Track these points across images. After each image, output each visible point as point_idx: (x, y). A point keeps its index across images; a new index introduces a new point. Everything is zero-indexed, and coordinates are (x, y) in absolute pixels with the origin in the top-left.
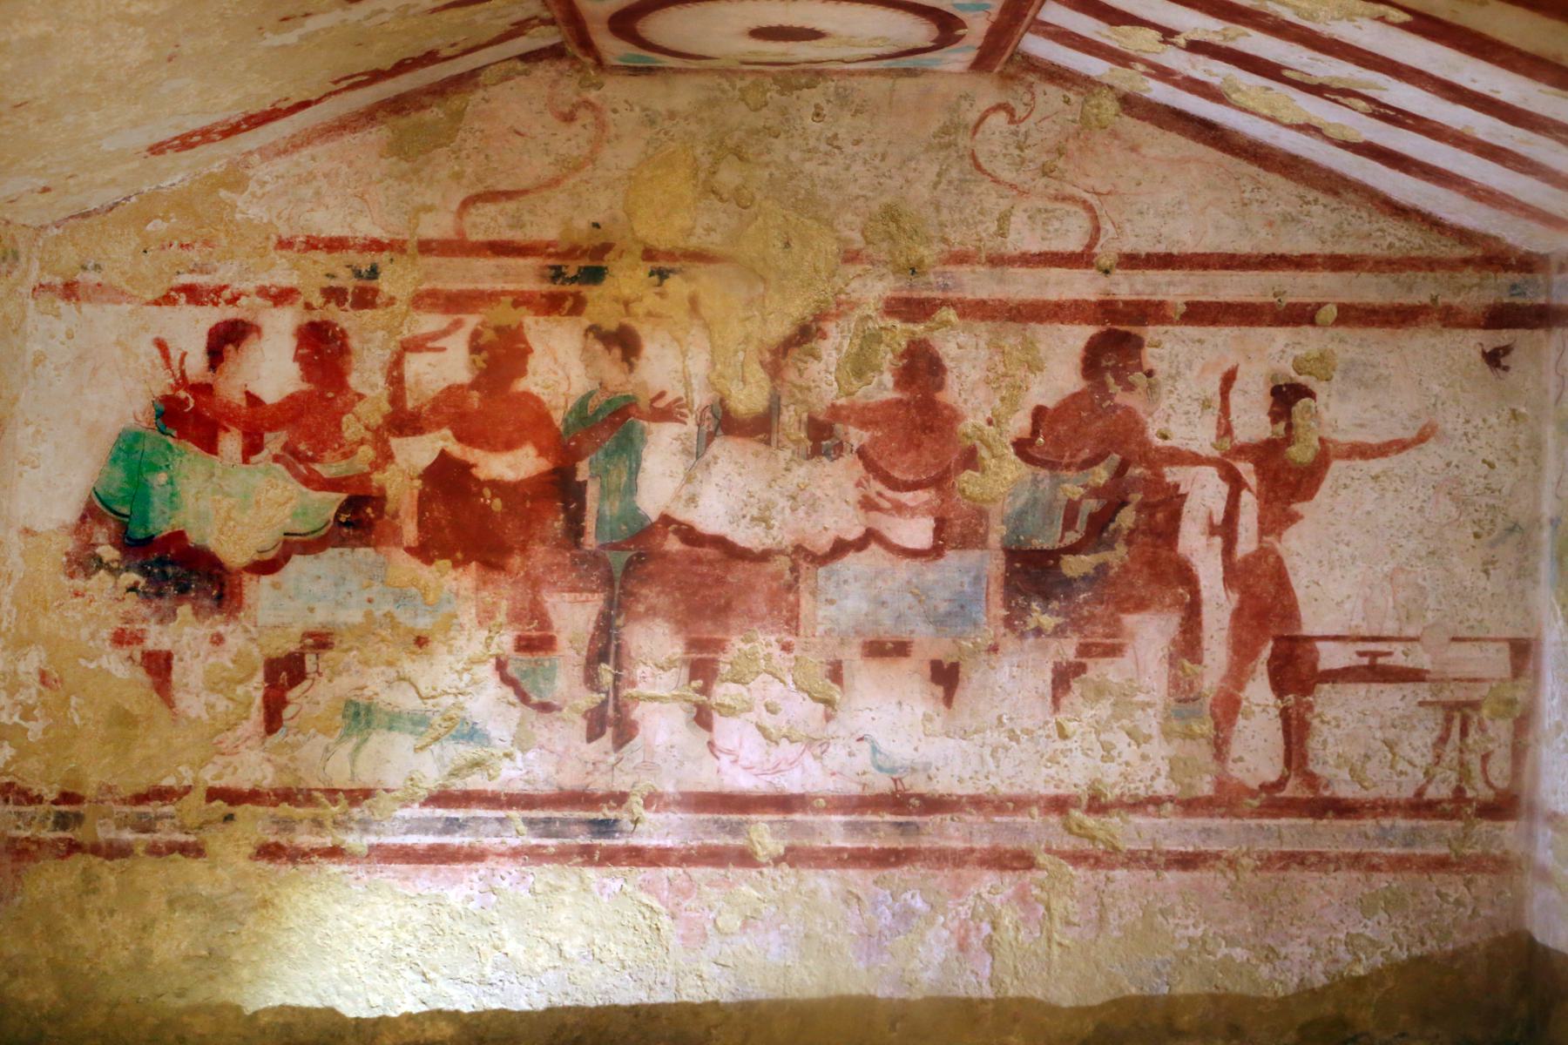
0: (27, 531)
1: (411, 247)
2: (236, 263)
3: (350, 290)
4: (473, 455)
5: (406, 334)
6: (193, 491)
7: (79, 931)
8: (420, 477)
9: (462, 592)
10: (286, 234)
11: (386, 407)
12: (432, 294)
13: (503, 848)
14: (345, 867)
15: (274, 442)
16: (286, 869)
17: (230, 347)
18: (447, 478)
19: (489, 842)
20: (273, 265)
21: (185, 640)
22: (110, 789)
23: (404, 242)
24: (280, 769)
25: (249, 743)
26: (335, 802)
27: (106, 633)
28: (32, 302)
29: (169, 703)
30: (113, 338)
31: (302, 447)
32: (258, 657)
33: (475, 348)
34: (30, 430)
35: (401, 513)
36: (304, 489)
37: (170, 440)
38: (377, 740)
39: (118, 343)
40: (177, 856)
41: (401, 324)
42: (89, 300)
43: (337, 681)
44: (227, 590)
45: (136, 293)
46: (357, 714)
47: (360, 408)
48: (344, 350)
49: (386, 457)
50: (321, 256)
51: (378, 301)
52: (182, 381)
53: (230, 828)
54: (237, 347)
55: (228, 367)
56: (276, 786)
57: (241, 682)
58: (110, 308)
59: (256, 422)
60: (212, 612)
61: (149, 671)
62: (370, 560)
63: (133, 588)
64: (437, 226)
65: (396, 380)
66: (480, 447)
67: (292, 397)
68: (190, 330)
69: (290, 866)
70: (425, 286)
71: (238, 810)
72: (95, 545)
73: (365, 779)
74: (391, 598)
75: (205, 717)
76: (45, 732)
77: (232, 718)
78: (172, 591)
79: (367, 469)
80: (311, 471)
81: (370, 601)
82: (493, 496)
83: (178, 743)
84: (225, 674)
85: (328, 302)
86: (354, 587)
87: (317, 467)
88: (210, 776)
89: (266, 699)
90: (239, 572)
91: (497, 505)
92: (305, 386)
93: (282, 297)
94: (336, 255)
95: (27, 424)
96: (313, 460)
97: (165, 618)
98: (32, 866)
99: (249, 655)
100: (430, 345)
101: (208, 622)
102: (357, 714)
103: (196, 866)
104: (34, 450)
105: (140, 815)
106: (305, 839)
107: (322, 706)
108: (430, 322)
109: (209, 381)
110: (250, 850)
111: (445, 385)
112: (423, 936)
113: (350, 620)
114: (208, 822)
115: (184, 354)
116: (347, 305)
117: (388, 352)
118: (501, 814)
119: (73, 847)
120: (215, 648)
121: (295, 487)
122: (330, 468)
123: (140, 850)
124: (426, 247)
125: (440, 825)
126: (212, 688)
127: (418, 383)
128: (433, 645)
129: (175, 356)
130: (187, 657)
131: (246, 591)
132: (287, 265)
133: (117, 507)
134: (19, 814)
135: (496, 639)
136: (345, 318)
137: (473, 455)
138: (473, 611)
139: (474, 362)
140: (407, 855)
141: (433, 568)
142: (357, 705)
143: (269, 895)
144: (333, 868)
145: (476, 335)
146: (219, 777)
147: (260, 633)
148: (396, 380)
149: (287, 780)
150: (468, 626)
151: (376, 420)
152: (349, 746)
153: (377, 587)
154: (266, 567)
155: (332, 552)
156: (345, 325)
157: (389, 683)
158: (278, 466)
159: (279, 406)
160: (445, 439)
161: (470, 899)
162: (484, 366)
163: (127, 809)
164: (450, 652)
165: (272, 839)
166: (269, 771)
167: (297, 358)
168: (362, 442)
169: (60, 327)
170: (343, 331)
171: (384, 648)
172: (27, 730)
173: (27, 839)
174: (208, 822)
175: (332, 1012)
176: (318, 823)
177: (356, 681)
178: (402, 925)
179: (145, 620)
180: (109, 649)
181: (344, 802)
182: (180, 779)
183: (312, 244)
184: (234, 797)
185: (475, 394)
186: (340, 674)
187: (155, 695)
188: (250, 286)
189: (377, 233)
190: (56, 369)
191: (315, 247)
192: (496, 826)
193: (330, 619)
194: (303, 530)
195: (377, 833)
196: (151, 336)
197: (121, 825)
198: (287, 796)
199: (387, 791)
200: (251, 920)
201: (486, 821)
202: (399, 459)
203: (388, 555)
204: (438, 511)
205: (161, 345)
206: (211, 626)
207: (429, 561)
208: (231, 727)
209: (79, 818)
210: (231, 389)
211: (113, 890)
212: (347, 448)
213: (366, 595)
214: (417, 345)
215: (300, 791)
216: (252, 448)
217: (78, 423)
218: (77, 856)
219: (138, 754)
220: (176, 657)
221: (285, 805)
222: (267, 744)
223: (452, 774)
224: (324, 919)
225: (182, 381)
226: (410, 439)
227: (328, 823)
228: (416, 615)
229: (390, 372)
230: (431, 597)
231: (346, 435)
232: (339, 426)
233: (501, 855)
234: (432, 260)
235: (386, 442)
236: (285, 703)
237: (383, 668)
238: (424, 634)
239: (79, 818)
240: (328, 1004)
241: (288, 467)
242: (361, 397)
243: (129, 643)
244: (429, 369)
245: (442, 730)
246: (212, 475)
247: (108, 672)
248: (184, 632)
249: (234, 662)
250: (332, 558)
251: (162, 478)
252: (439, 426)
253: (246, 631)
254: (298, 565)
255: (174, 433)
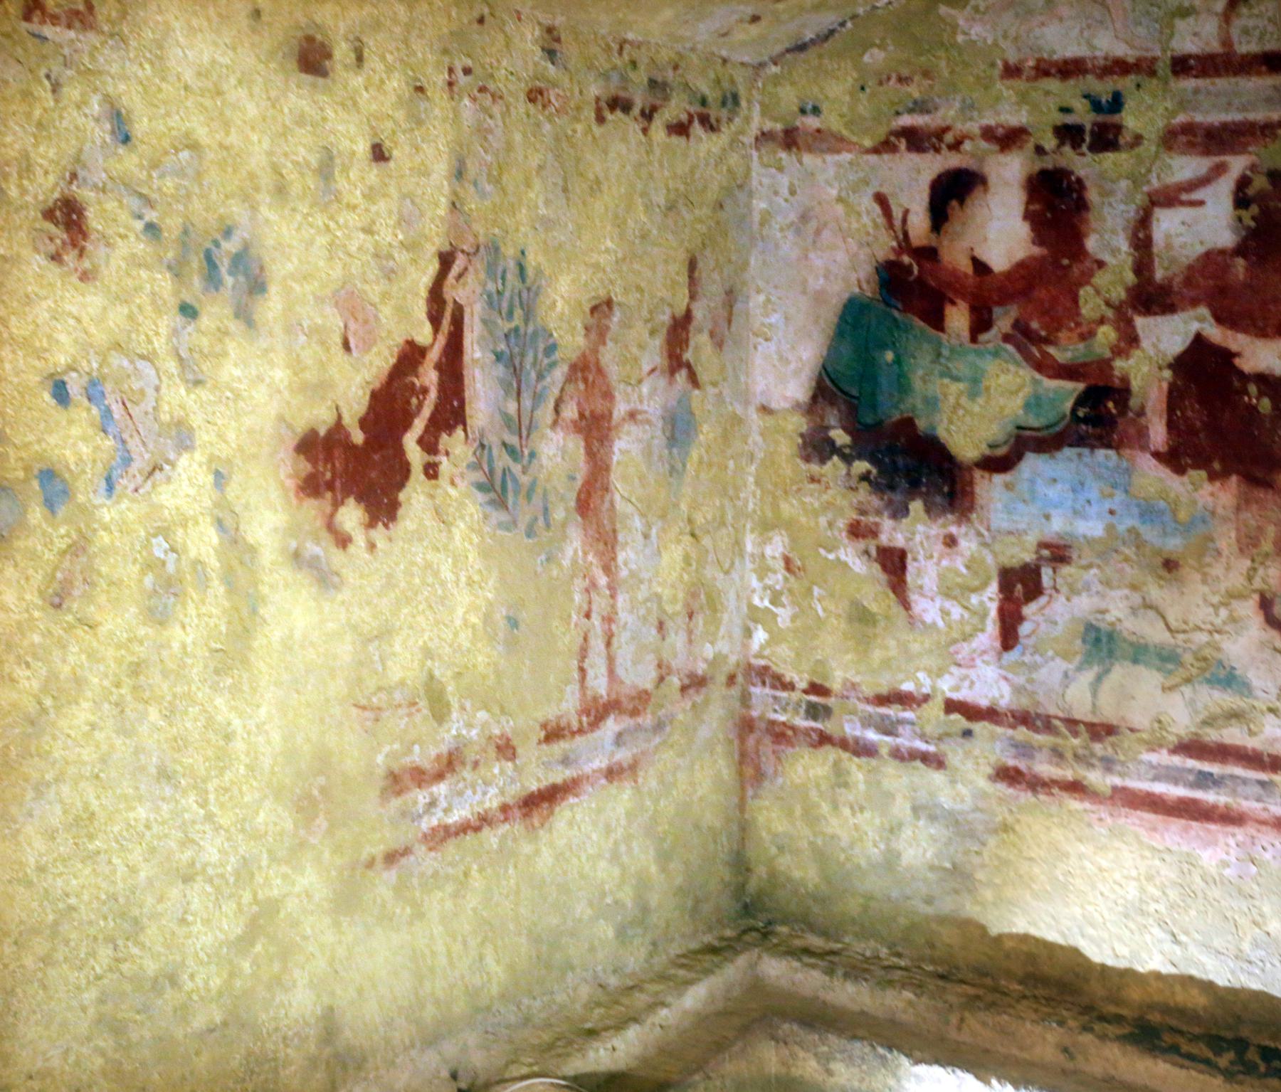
0: (765, 410)
1: (1163, 68)
2: (958, 98)
3: (1088, 127)
4: (1236, 341)
5: (1155, 183)
6: (920, 372)
7: (834, 821)
8: (1170, 366)
9: (1220, 511)
10: (1013, 58)
11: (1130, 278)
12: (1188, 129)
13: (1265, 815)
14: (1087, 805)
15: (1004, 320)
16: (1026, 797)
17: (954, 203)
18: (1202, 370)
19: (1248, 805)
20: (998, 99)
21: (918, 538)
22: (854, 686)
23: (1154, 60)
24: (1018, 690)
25: (986, 657)
26: (1076, 734)
27: (842, 523)
28: (755, 154)
29: (906, 605)
30: (834, 192)
31: (1035, 325)
32: (991, 563)
33: (1241, 200)
34: (761, 298)
35: (1148, 411)
36: (1038, 376)
37: (896, 314)
38: (1119, 672)
39: (840, 199)
40: (918, 763)
41: (1149, 171)
42: (810, 149)
43: (1075, 600)
44: (958, 487)
45: (854, 139)
46: (1098, 640)
47: (1101, 279)
48: (1082, 205)
49: (1130, 340)
50: (1053, 84)
51: (1121, 141)
52: (905, 244)
53: (968, 744)
54: (962, 202)
55: (953, 226)
56: (1014, 707)
57: (974, 590)
58: (830, 158)
59: (986, 292)
60: (944, 511)
61: (884, 568)
62: (1111, 464)
63: (865, 477)
64: (1195, 37)
65: (1142, 243)
66: (1246, 331)
67: (1021, 265)
68: (912, 179)
69: (1029, 794)
70: (1181, 118)
71: (980, 727)
72: (828, 428)
73: (1108, 713)
74: (1136, 511)
75: (941, 623)
76: (794, 618)
77: (968, 629)
78: (904, 484)
79: (1108, 354)
80: (1045, 355)
81: (1112, 512)
82: (1261, 394)
83: (915, 647)
84: (959, 580)
85: (1062, 144)
86: (1094, 495)
87: (1051, 350)
88: (946, 686)
89: (1001, 611)
90: (969, 469)
91: (1265, 405)
92: (1037, 251)
93: (1009, 139)
94: (1072, 82)
95: (759, 291)
96: (1047, 341)
97: (899, 512)
98: (789, 750)
99: (983, 561)
100: (1184, 197)
101: (941, 521)
102: (1098, 640)
103: (938, 777)
104: (767, 321)
105: (884, 717)
106: (1045, 768)
107: (1060, 628)
108: (1186, 167)
109: (934, 244)
110: (990, 771)
111: (1200, 250)
112: (1173, 894)
113: (1089, 534)
114: (948, 735)
115: (906, 212)
116: (1084, 148)
117: (1132, 208)
118: (1263, 776)
119: (824, 739)
120: (948, 550)
121: (1027, 373)
122: (1062, 354)
123: (884, 751)
124: (1181, 66)
125: (1191, 778)
126: (947, 593)
127: (1169, 246)
128: (1185, 571)
129: (897, 214)
130: (921, 557)
131: (978, 490)
132: (1014, 99)
133: (847, 388)
134: (775, 698)
135: (1261, 572)
136: (1083, 164)
137: (1236, 341)
138: (1233, 535)
139: (1240, 219)
140: (1154, 804)
141: (1185, 479)
142: (1098, 630)
143: (1010, 819)
144: (1075, 804)
145: (1243, 183)
146: (957, 688)
147: (994, 538)
148: (1142, 243)
149: (1024, 703)
150: (1226, 552)
151: (1119, 294)
152: (1088, 676)
153: (1120, 496)
154: (999, 463)
155: (1068, 452)
156: (1081, 172)
157: (1134, 611)
158: (1010, 347)
159: (1008, 275)
160: (1201, 319)
161: (1225, 864)
162: (1252, 224)
163: (870, 709)
164: (1204, 582)
165: (1011, 762)
166: (1006, 690)
167: (1028, 216)
168: (1102, 321)
169: (784, 181)
170: (1079, 181)
171: (1128, 569)
172: (775, 615)
173: (784, 724)
174: (948, 735)
175: (1075, 952)
176: (1058, 754)
177: (1096, 602)
178: (1150, 878)
179: (878, 512)
180: (846, 541)
181: (1085, 735)
182: (918, 684)
183: (1044, 70)
184: (971, 712)
185: (1240, 263)
186: (1078, 593)
187: (892, 595)
188: (974, 127)
189: (1120, 50)
190: (782, 230)
191: (1047, 74)
192: (1257, 790)
193: (1068, 529)
194: (1036, 424)
195: (1122, 775)
196: (870, 191)
197: (867, 722)
198: (1024, 719)
199: (1132, 730)
200: (992, 841)
201: (1245, 782)
202: (1145, 343)
203: (1132, 460)
204: (1193, 412)
205: (881, 200)
206: (944, 526)
207: (1180, 470)
208: (966, 638)
209: (827, 711)
210: (956, 256)
211: (862, 787)
212: (1084, 329)
213: (1107, 505)
214: (1169, 198)
215: (1038, 716)
216: (980, 324)
217: (804, 292)
218: (828, 747)
219: (877, 655)
220: (909, 556)
221: (1023, 729)
222: (1004, 662)
223: (1205, 723)
224: (1067, 855)
225: (905, 244)
226: (1159, 319)
227: (1069, 755)
228: (1165, 534)
229: (1135, 235)
230: (1182, 515)
231: (1084, 311)
232: (1075, 300)
233: (1263, 823)
234: (1189, 83)
235: (1130, 322)
236: (1021, 619)
237: (1126, 591)
238: (1174, 557)
239: (827, 711)
240: (1072, 942)
241: (1019, 348)
242: (1101, 264)
243: (864, 537)
244: (1182, 229)
245: (1194, 671)
246: (939, 355)
247: (845, 565)
248: (916, 531)
249: (968, 567)
250: (1070, 460)
251: (889, 356)
252: (1194, 303)
253: (979, 534)
254: (1032, 464)
255: (900, 306)
